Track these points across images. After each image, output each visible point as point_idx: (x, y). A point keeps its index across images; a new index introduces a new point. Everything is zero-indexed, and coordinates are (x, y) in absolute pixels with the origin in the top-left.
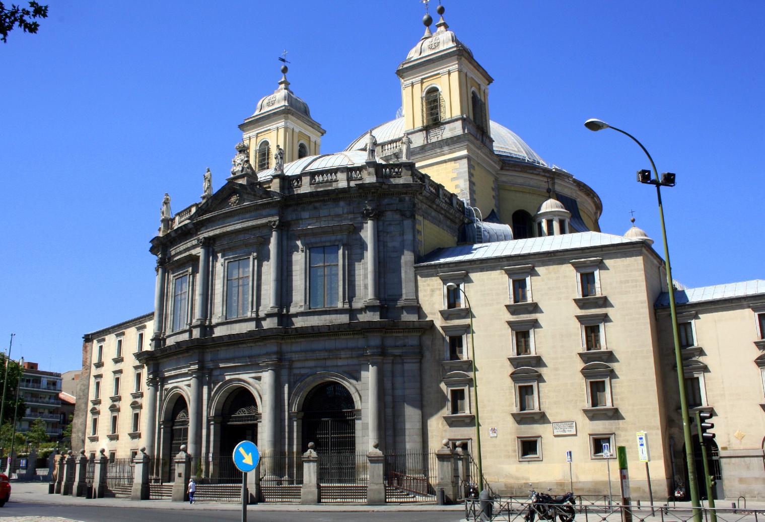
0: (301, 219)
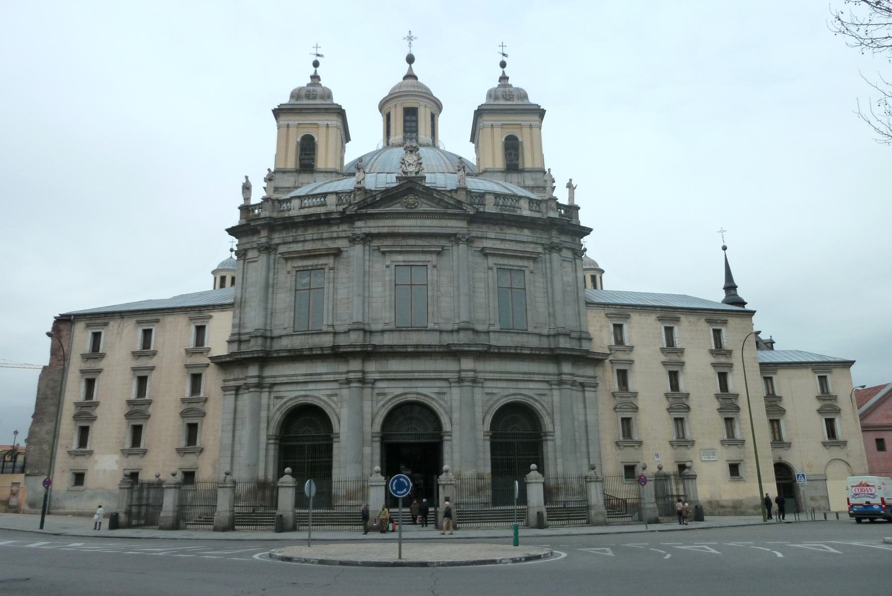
0: (486, 238)
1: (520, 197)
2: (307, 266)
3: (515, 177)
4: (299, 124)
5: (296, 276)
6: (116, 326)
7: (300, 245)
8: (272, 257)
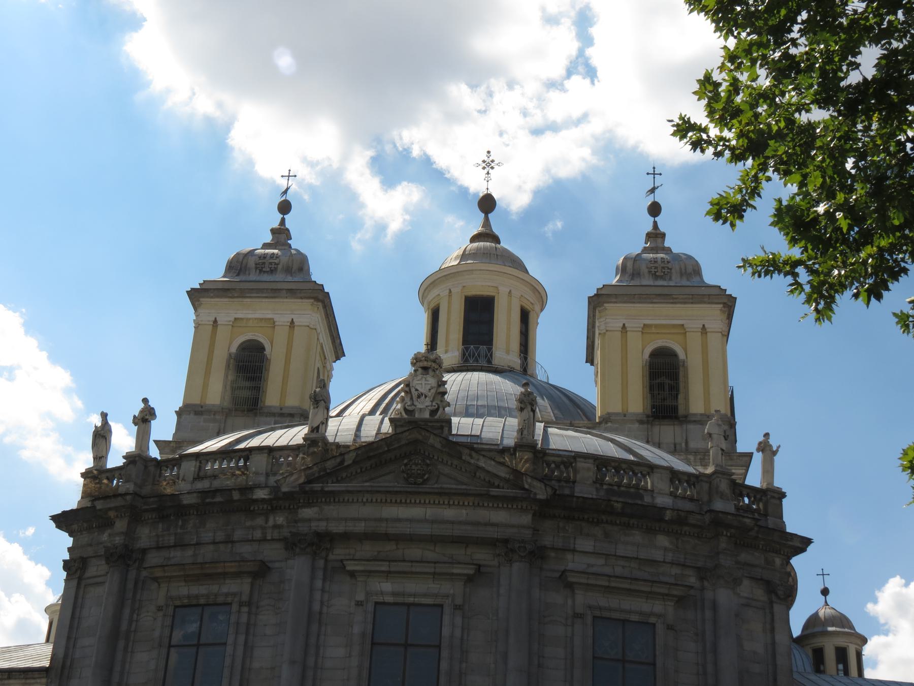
0: (574, 551)
1: (652, 468)
2: (197, 597)
3: (668, 432)
4: (236, 319)
5: (174, 616)
7: (189, 552)
8: (132, 574)
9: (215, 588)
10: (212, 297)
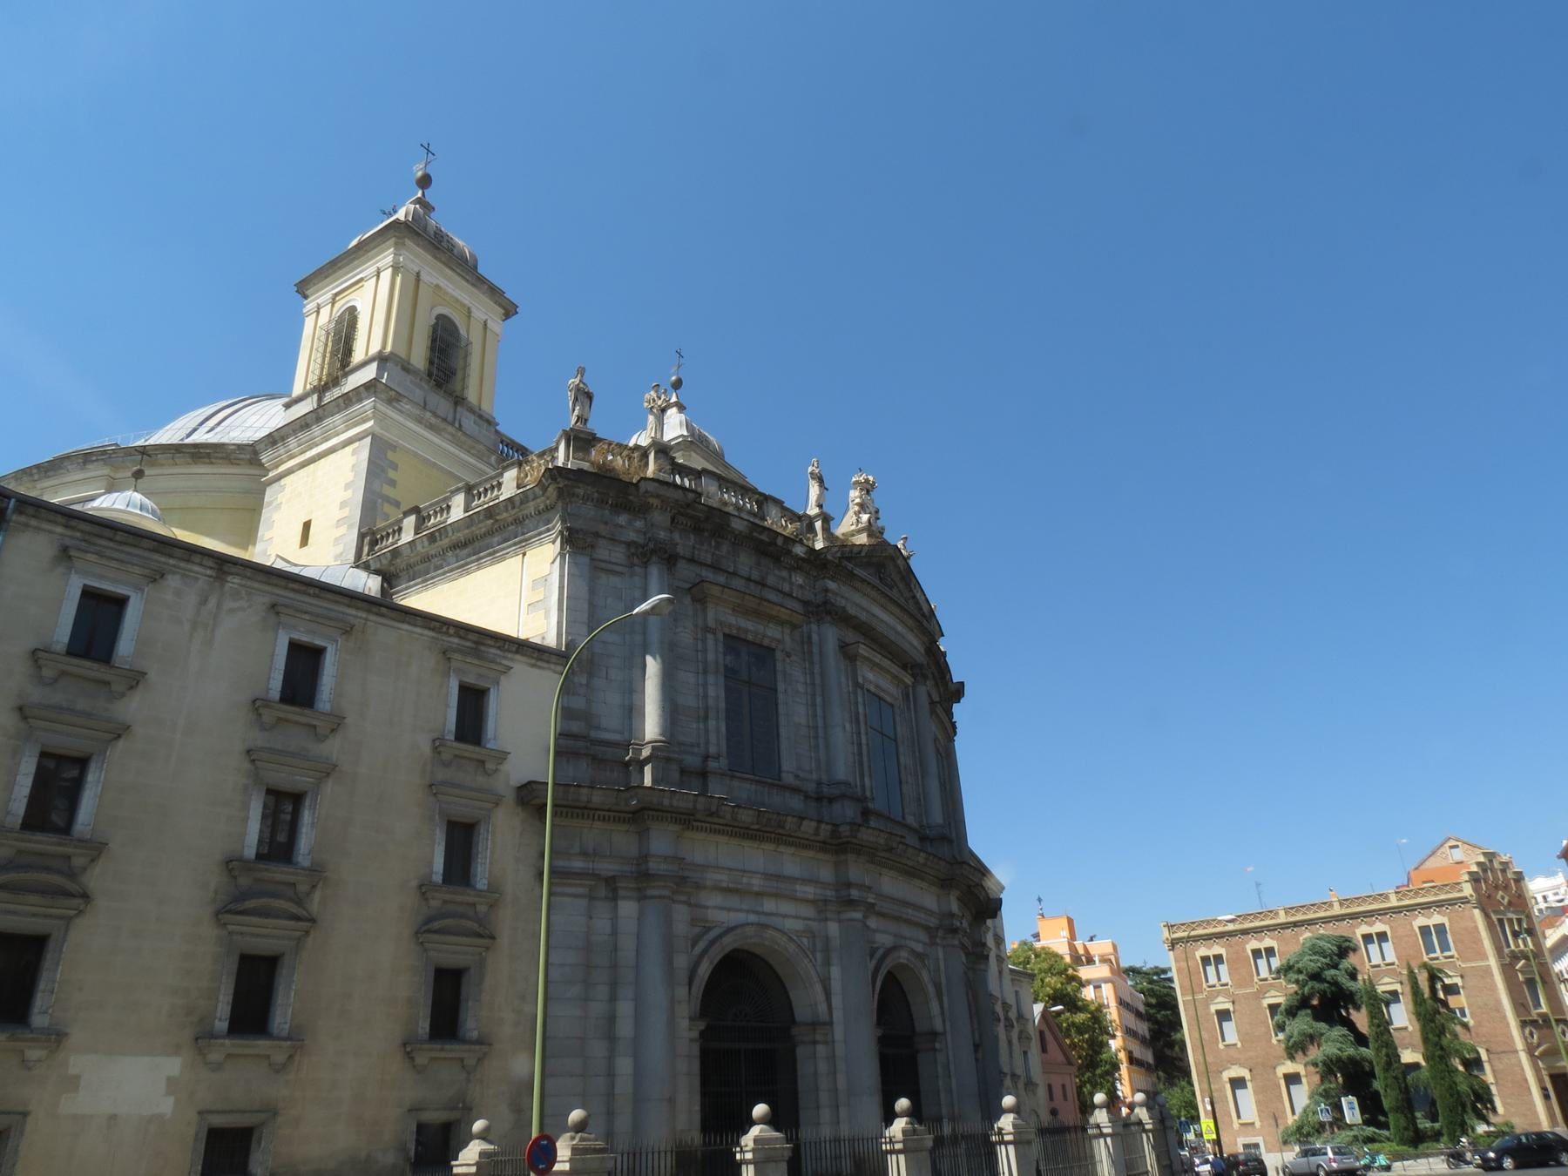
2: (747, 631)
4: (437, 286)
6: (191, 599)
7: (722, 579)
9: (761, 628)
10: (418, 245)
